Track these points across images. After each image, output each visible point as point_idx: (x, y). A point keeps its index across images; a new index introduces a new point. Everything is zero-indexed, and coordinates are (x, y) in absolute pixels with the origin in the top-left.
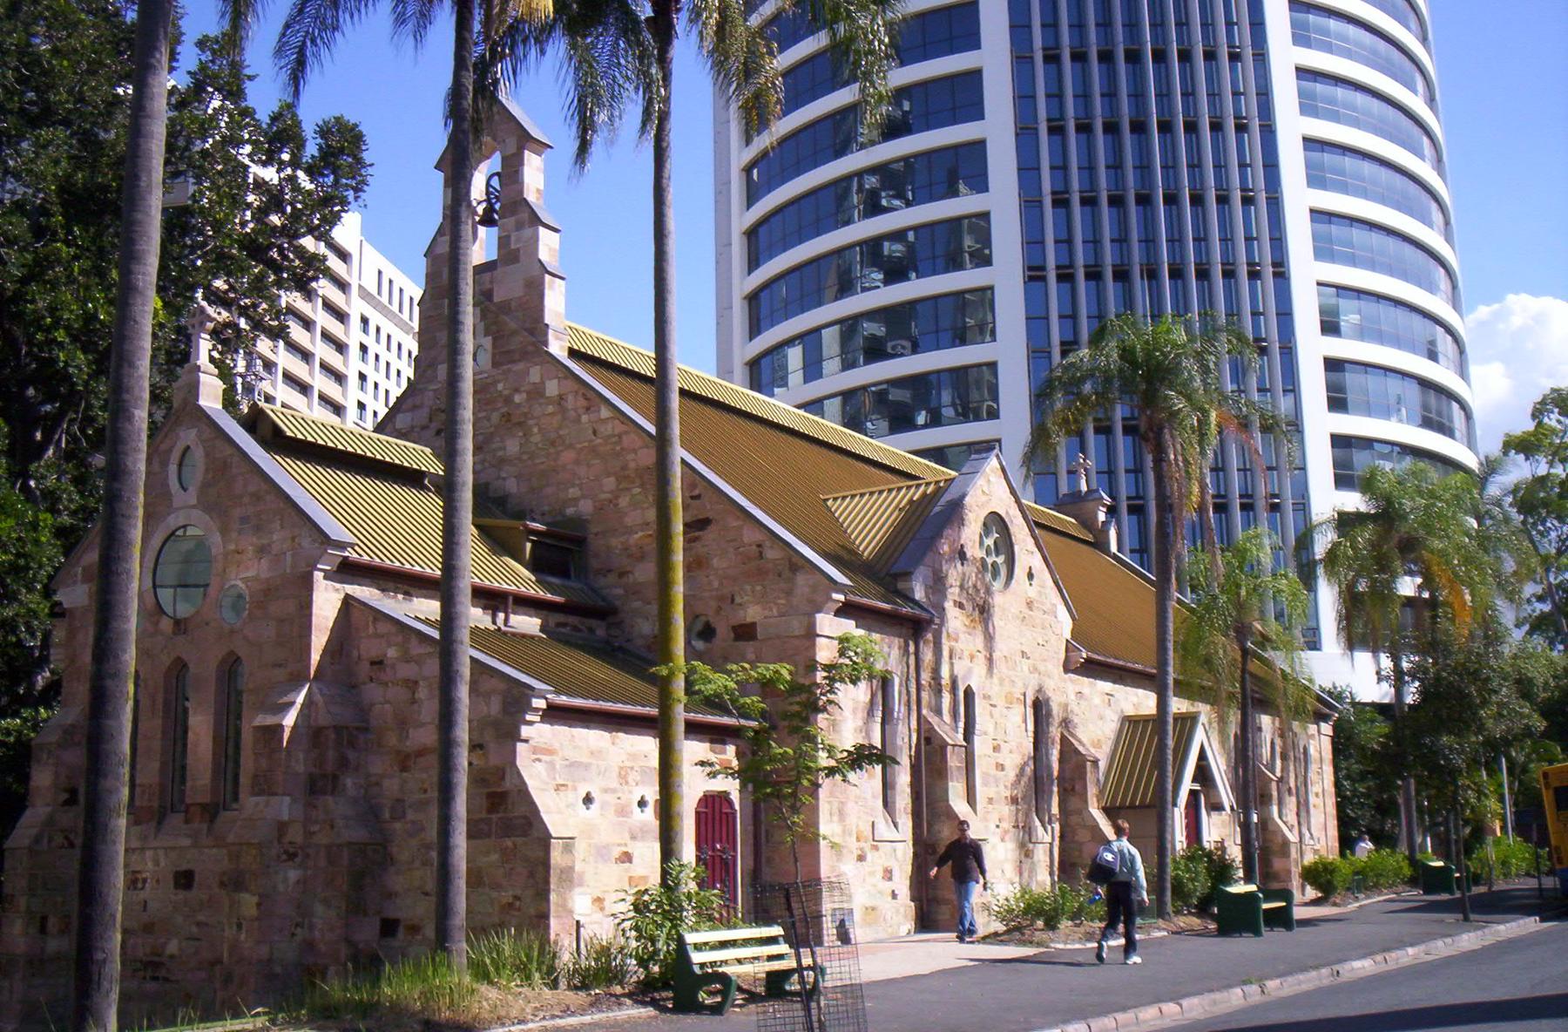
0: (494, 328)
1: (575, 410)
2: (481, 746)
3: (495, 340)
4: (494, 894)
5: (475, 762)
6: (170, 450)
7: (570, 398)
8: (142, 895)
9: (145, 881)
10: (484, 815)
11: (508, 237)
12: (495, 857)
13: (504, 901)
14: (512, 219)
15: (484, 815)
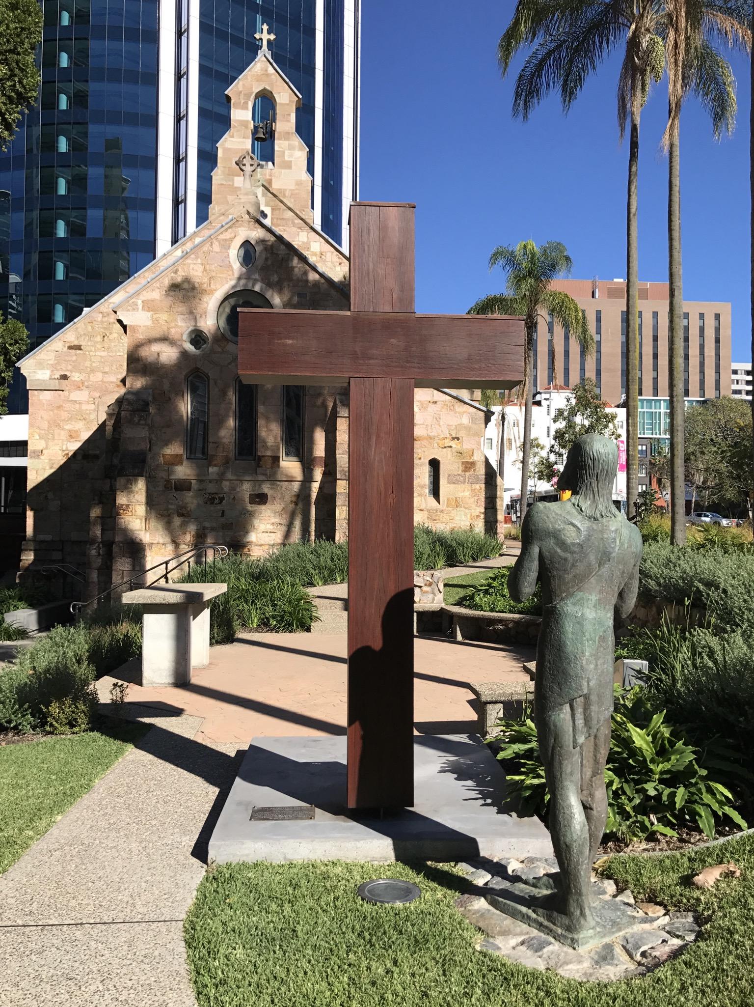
0: (272, 203)
1: (332, 262)
2: (458, 439)
3: (273, 210)
4: (467, 511)
5: (454, 446)
6: (231, 240)
7: (329, 254)
8: (219, 507)
9: (222, 500)
10: (460, 472)
11: (284, 152)
12: (467, 493)
13: (474, 514)
14: (286, 142)
15: (460, 472)
